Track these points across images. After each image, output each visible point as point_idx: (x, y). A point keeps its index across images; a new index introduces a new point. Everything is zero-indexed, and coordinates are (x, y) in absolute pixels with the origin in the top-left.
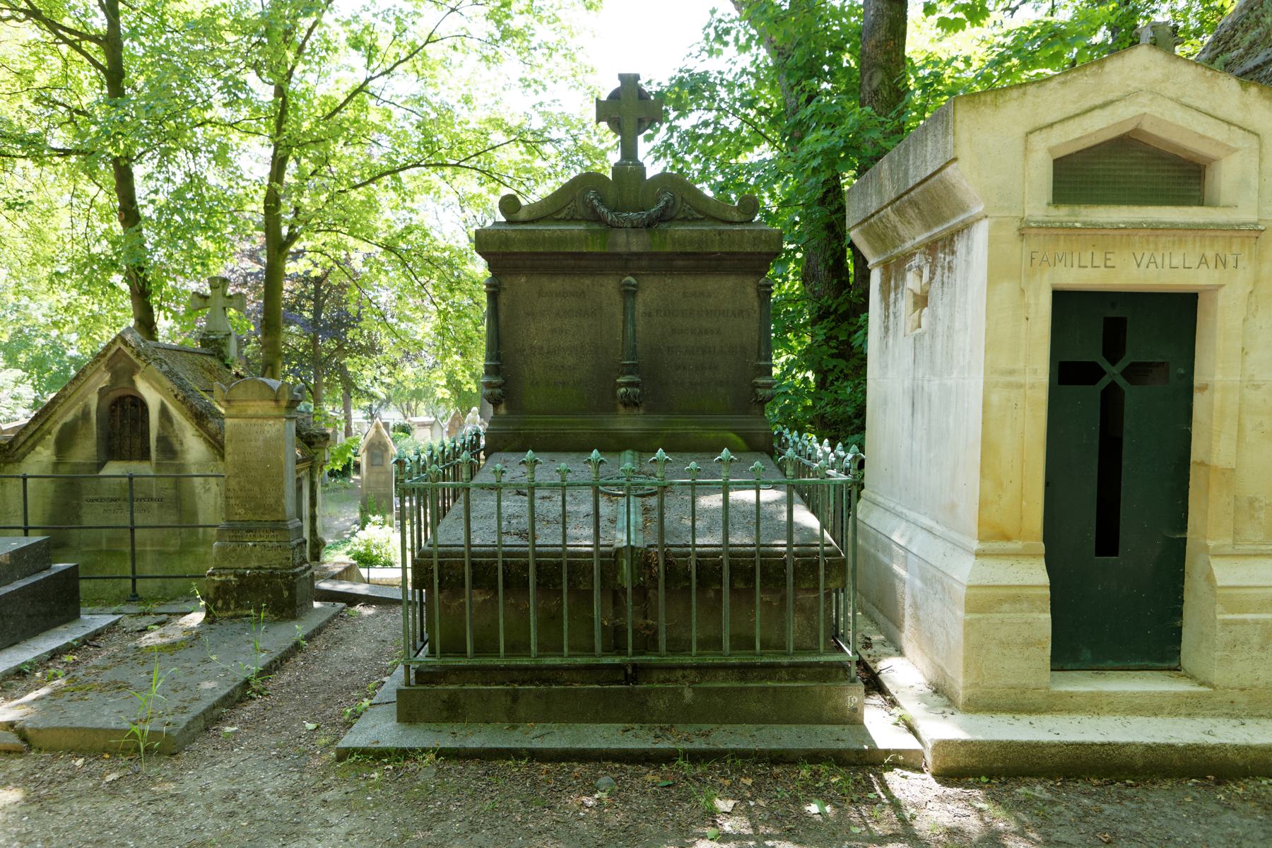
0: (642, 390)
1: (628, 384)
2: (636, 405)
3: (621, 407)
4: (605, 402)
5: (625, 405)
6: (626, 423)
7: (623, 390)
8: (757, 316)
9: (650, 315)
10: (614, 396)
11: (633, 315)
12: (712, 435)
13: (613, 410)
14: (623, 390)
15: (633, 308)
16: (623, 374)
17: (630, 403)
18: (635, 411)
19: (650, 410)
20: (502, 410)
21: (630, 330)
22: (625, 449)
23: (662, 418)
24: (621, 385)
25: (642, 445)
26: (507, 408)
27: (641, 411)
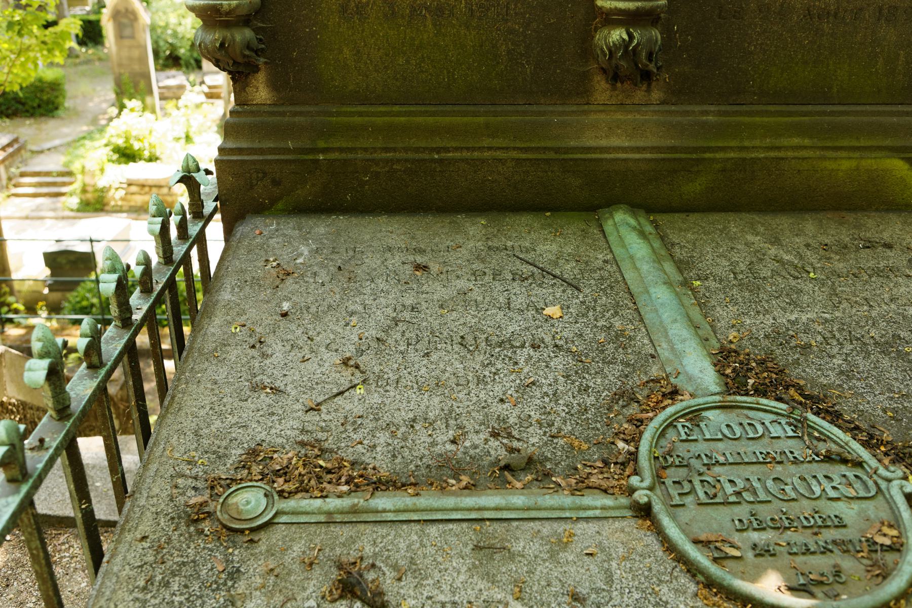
0: (667, 31)
3: (600, 84)
5: (615, 77)
6: (617, 130)
7: (617, 35)
10: (586, 50)
12: (844, 165)
13: (579, 91)
14: (617, 35)
18: (640, 95)
19: (682, 92)
20: (261, 93)
22: (611, 203)
23: (710, 114)
26: (274, 85)
27: (656, 95)
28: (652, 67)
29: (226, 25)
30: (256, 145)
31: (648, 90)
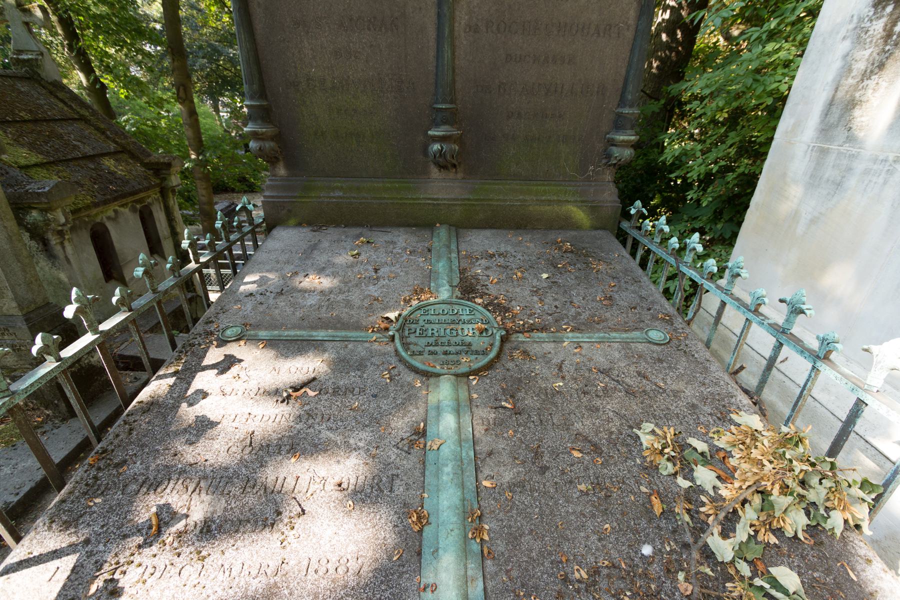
1: (442, 139)
2: (454, 166)
4: (411, 163)
7: (436, 147)
8: (630, 34)
9: (476, 30)
11: (452, 31)
14: (436, 147)
15: (453, 19)
16: (436, 124)
17: (444, 164)
18: (451, 175)
21: (447, 54)
24: (435, 139)
25: (462, 224)
26: (288, 166)
27: (460, 175)
28: (454, 162)
29: (263, 139)
30: (280, 194)
31: (456, 172)
